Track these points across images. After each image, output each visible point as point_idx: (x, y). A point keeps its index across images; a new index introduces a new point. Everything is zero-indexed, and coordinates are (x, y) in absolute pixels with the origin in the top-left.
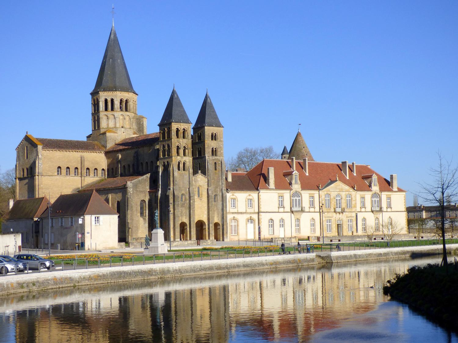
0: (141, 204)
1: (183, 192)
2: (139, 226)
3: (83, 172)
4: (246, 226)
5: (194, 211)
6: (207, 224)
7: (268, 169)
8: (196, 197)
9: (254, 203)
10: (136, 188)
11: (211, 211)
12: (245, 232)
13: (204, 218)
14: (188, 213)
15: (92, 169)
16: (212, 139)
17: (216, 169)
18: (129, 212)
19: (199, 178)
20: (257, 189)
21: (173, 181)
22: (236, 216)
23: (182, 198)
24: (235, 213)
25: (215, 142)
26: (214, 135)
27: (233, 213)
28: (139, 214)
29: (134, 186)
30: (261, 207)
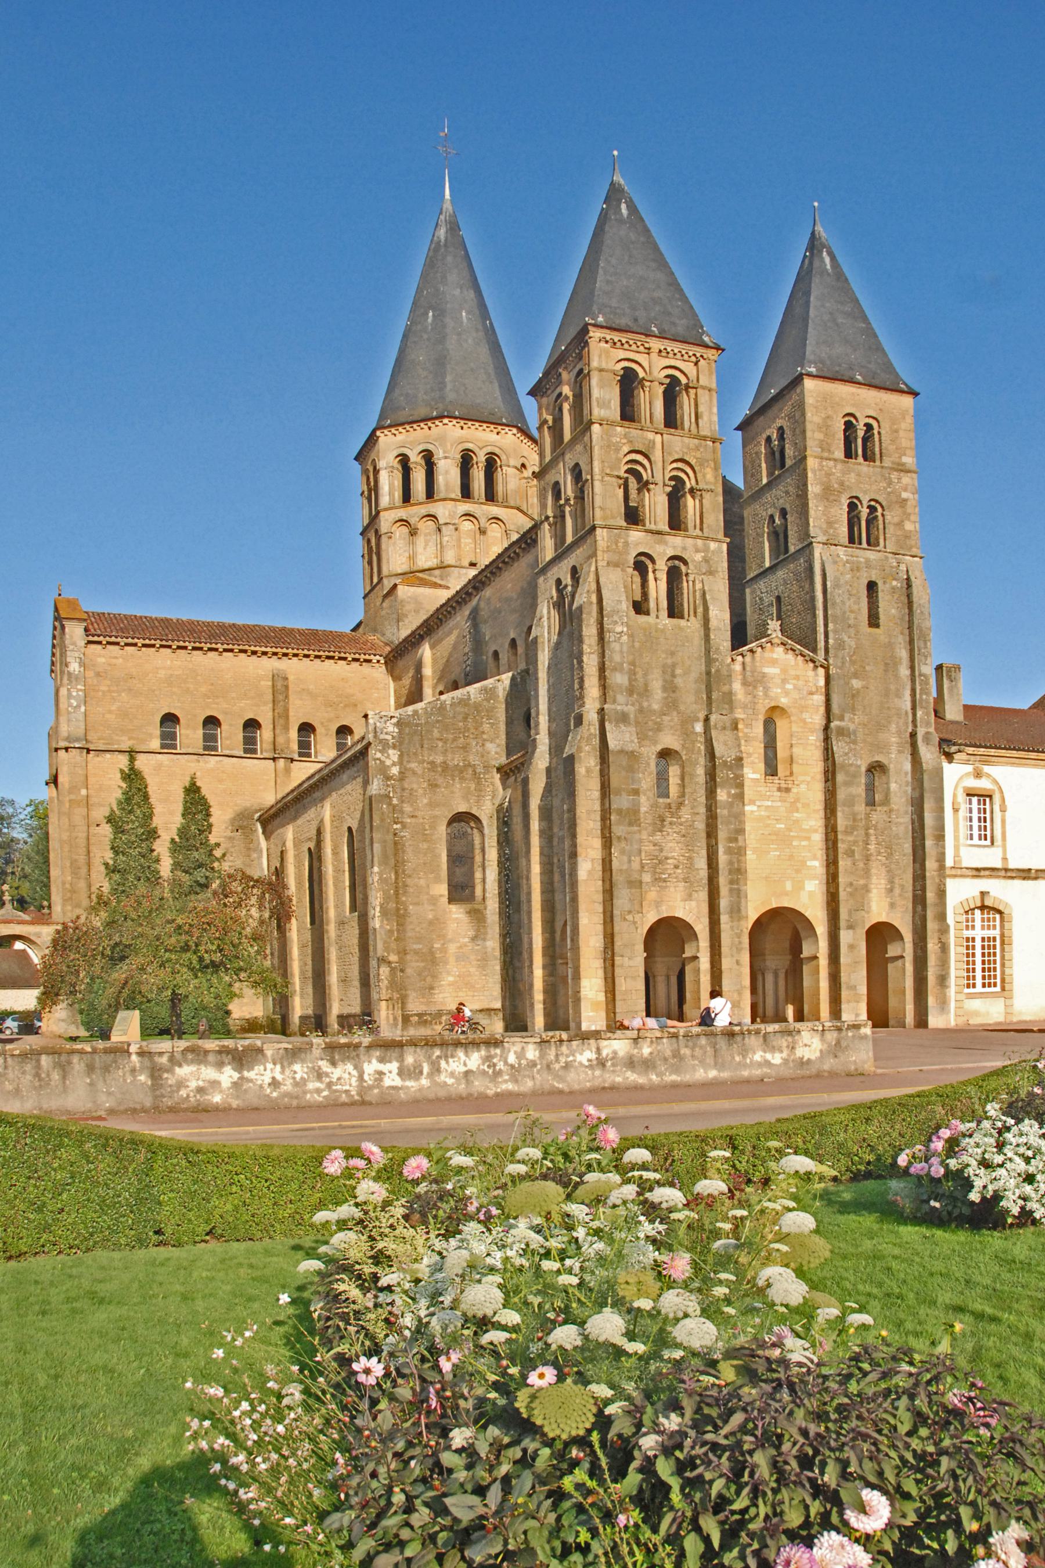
0: (453, 840)
1: (669, 740)
3: (280, 740)
5: (741, 852)
6: (821, 929)
8: (753, 772)
11: (850, 853)
13: (804, 898)
14: (702, 863)
15: (327, 730)
18: (380, 874)
21: (602, 669)
23: (662, 779)
28: (442, 889)
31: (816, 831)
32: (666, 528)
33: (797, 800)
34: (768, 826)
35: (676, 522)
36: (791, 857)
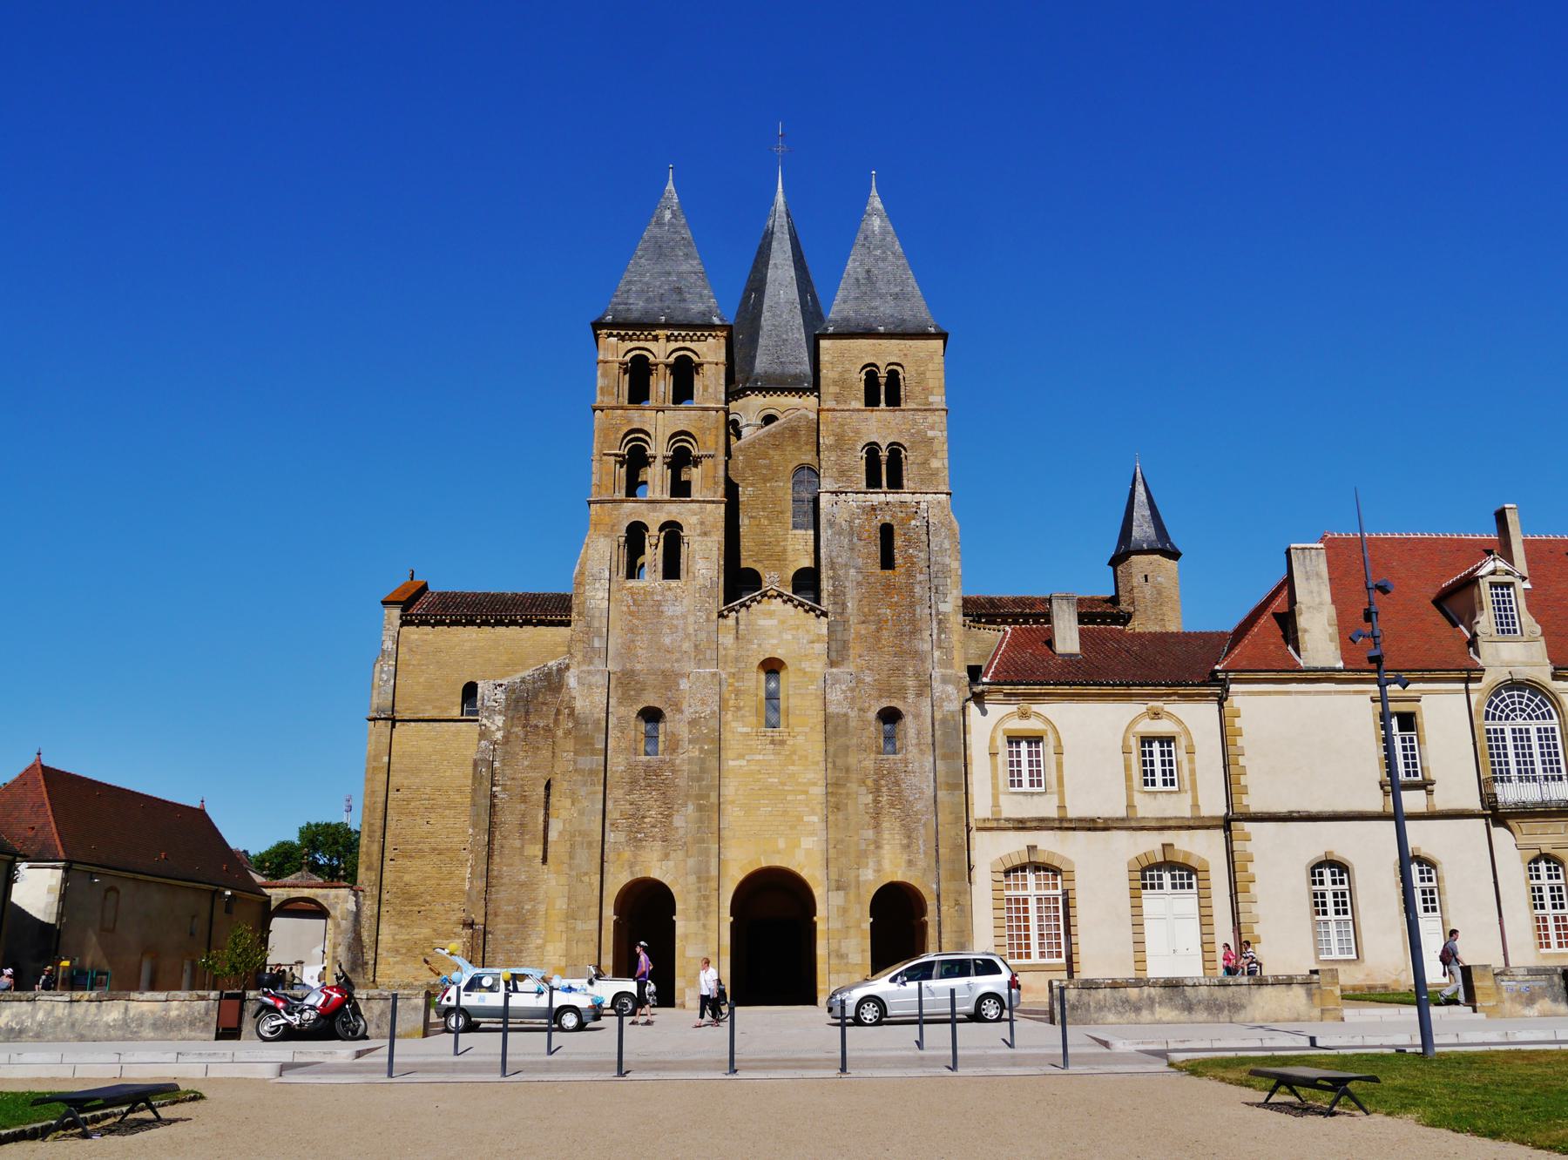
1: (651, 700)
2: (534, 912)
4: (1137, 908)
7: (1288, 552)
9: (1191, 761)
10: (527, 713)
12: (1130, 948)
16: (871, 400)
17: (887, 561)
19: (771, 614)
20: (1213, 679)
22: (1050, 844)
24: (1042, 824)
25: (887, 414)
26: (883, 381)
27: (1021, 825)
29: (517, 701)
30: (1243, 781)
31: (815, 784)
32: (667, 497)
33: (794, 752)
34: (759, 780)
35: (680, 489)
36: (785, 812)
